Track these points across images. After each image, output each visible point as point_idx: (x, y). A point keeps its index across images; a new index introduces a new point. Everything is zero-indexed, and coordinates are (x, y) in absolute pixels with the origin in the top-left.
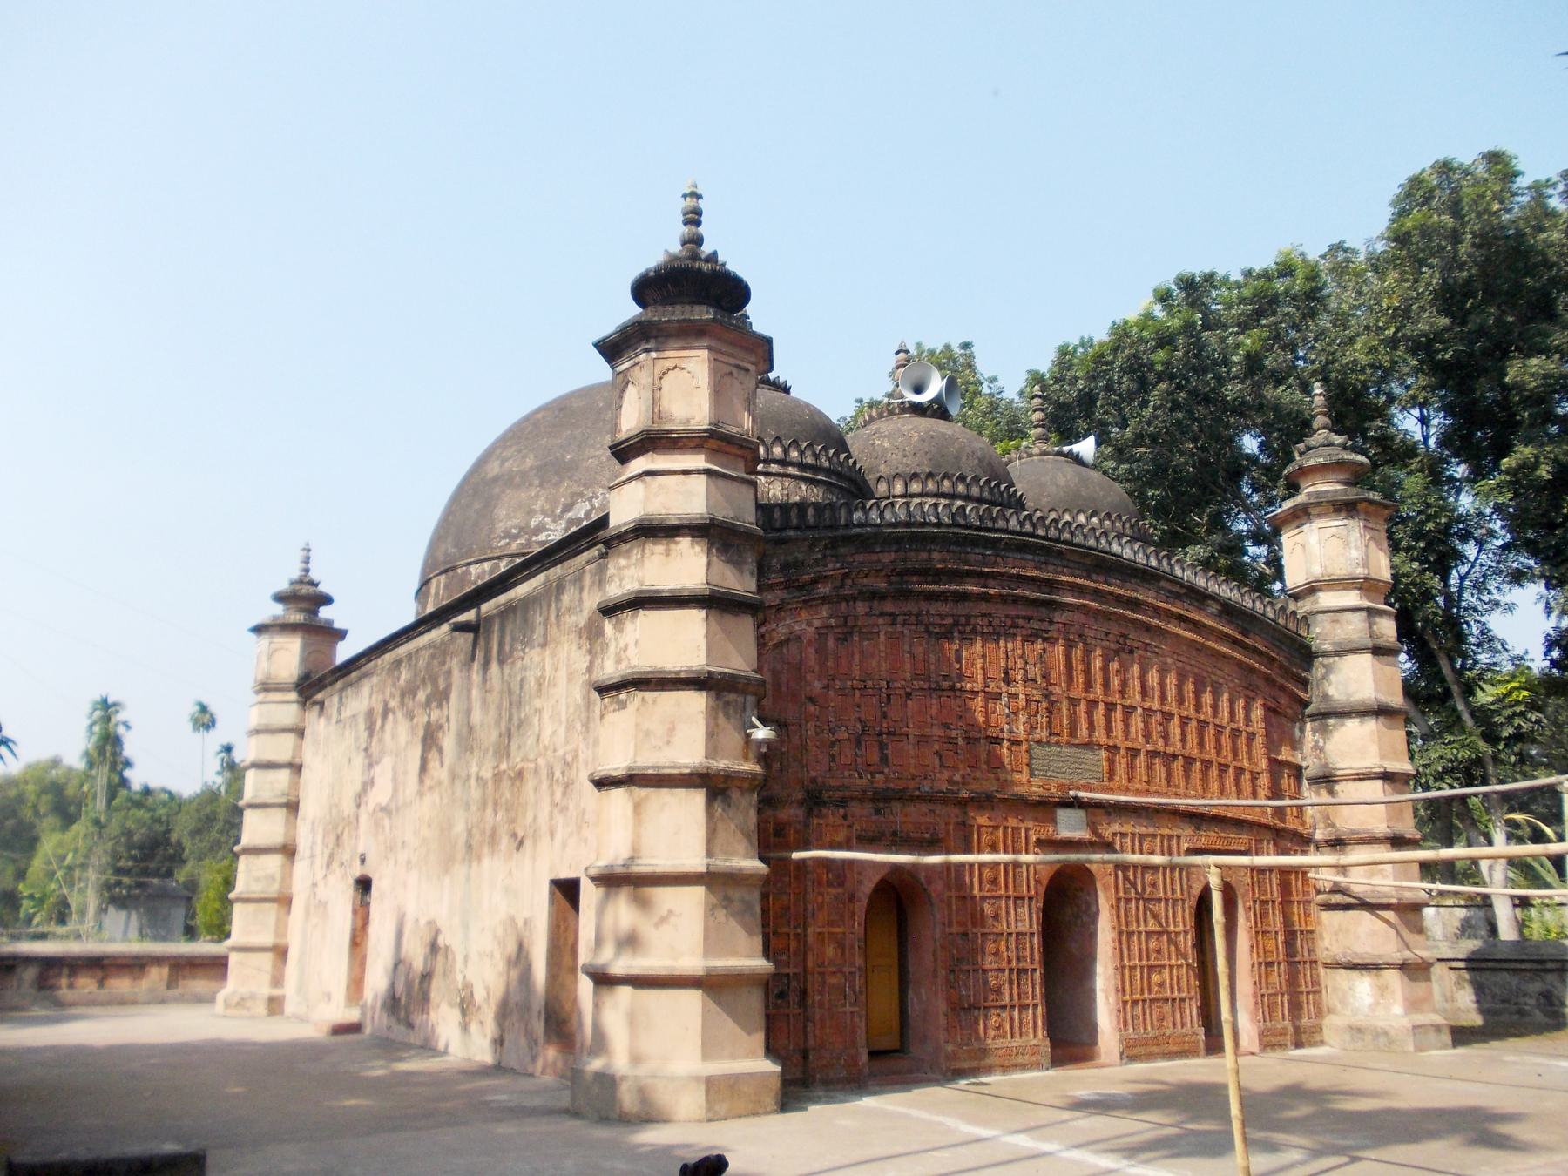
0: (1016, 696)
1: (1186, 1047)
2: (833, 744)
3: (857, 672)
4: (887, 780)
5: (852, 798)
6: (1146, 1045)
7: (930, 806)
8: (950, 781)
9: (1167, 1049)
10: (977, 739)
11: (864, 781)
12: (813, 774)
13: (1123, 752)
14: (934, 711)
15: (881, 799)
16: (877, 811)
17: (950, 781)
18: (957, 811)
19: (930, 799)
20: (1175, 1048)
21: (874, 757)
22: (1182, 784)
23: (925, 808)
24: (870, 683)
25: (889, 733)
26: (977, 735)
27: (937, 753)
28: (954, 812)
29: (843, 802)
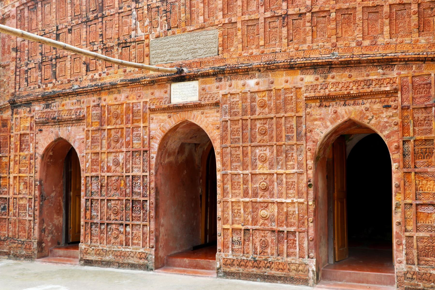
0: (142, 8)
1: (293, 274)
2: (26, 72)
3: (40, 26)
4: (54, 86)
5: (33, 100)
6: (246, 266)
7: (79, 98)
8: (93, 80)
9: (268, 272)
10: (112, 47)
11: (41, 89)
12: (13, 91)
13: (239, 25)
14: (84, 36)
15: (48, 99)
16: (48, 106)
17: (93, 80)
18: (95, 98)
19: (76, 93)
20: (279, 273)
21: (48, 73)
22: (309, 38)
23: (74, 100)
24: (47, 30)
25: (56, 58)
26: (111, 44)
27: (85, 63)
28: (92, 100)
29: (28, 103)
